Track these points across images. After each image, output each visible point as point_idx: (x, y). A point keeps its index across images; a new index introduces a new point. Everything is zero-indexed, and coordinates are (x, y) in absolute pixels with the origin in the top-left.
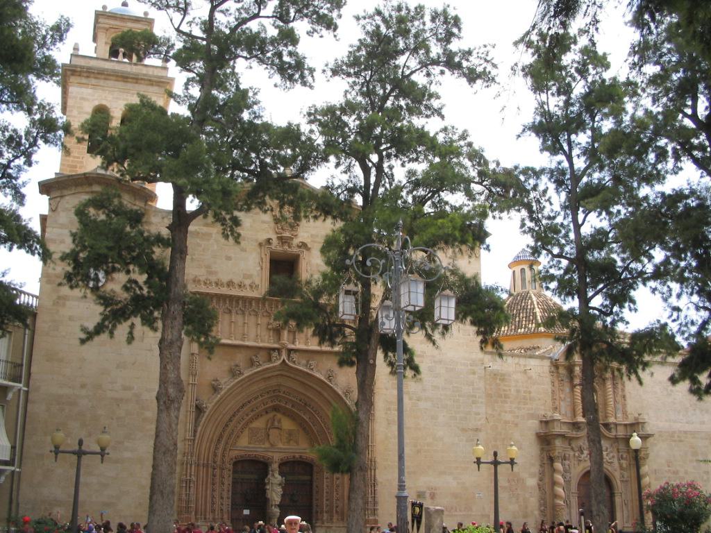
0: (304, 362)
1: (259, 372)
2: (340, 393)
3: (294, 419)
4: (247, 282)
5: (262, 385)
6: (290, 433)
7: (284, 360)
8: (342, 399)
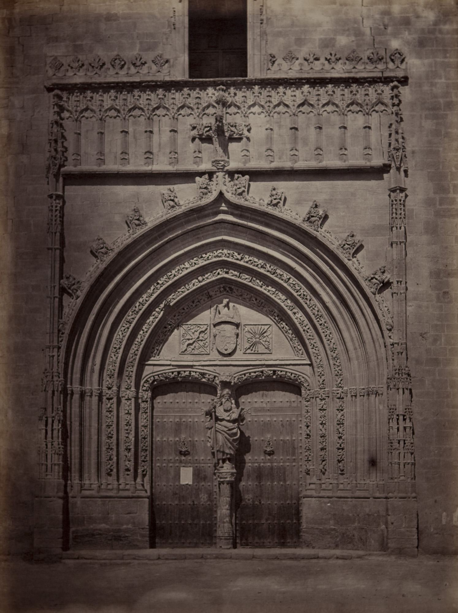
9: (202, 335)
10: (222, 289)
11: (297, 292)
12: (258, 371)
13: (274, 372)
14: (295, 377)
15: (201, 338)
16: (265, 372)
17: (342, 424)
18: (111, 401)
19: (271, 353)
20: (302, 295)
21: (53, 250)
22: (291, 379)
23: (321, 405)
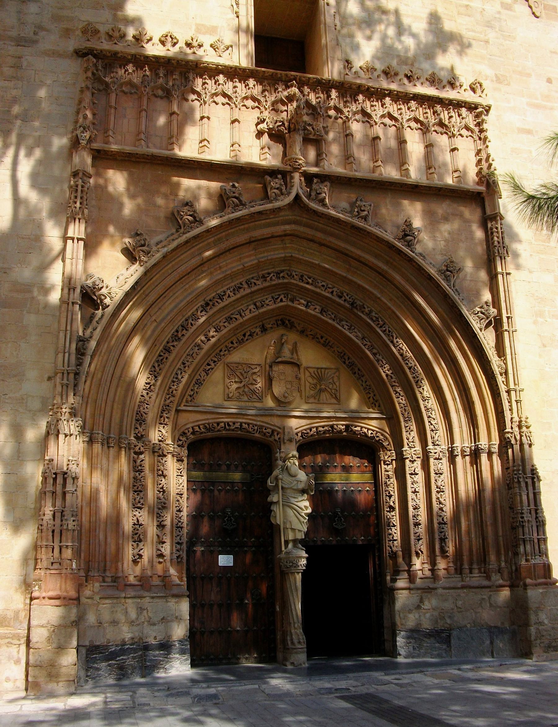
0: (344, 205)
2: (433, 272)
3: (326, 345)
4: (207, 40)
5: (250, 258)
6: (319, 376)
7: (297, 197)
8: (438, 286)
10: (279, 322)
11: (381, 327)
12: (327, 426)
14: (372, 433)
16: (335, 426)
17: (443, 492)
21: (76, 241)
23: (413, 469)
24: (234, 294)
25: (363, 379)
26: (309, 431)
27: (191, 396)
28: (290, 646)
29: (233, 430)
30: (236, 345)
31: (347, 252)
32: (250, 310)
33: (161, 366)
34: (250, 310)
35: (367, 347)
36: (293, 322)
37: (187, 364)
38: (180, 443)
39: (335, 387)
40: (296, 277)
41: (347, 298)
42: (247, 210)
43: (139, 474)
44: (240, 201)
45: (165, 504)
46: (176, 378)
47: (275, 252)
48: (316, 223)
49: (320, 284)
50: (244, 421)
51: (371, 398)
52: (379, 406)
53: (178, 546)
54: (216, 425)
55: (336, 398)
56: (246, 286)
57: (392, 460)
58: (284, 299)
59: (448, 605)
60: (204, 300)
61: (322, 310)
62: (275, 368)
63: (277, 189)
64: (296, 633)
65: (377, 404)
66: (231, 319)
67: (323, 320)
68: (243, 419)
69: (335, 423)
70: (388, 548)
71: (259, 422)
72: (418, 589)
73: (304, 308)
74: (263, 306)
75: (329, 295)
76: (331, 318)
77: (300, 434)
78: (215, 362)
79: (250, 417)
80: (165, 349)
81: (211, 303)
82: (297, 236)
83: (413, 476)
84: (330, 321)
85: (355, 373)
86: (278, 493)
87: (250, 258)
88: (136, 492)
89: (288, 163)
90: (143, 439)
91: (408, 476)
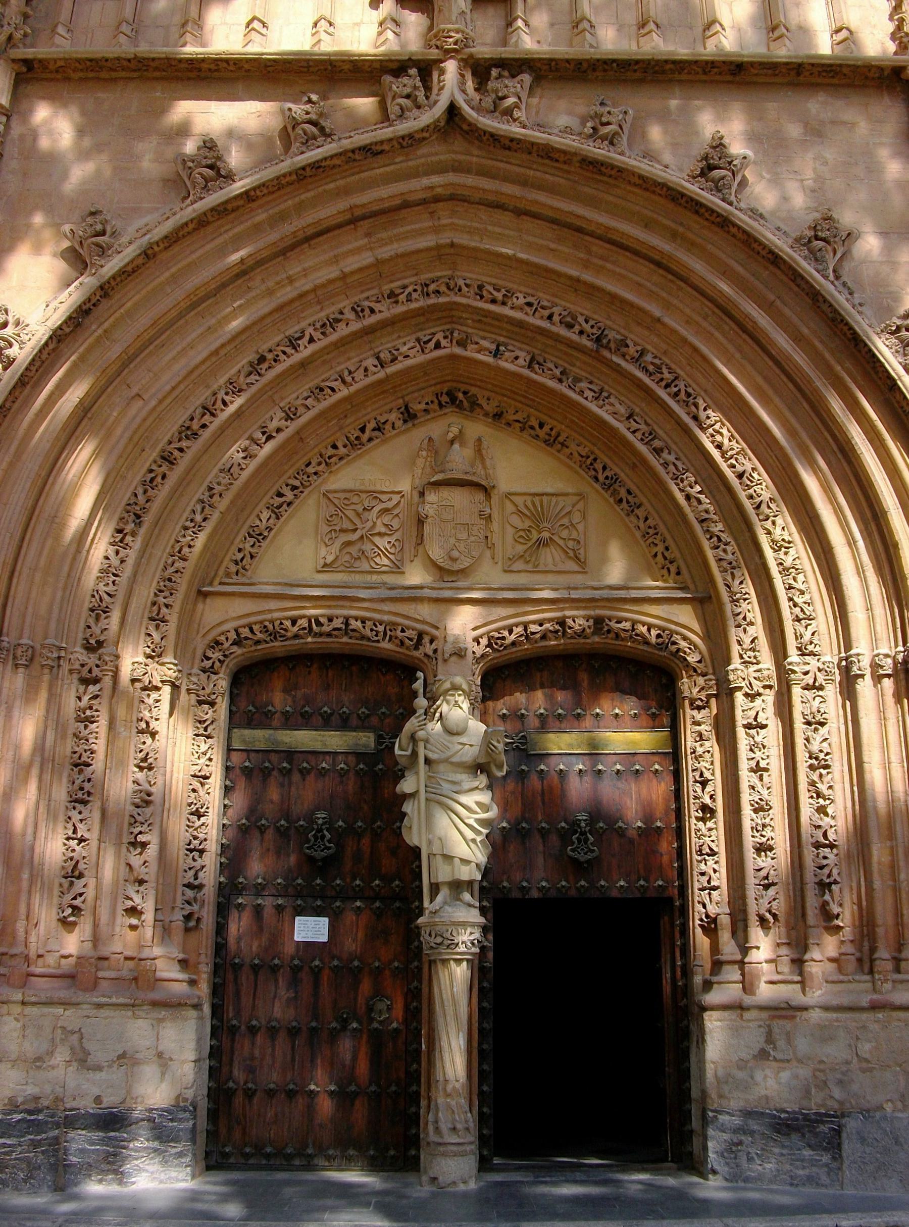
1: (316, 166)
2: (782, 245)
3: (552, 442)
7: (452, 110)
8: (795, 276)
9: (386, 519)
10: (445, 399)
11: (667, 386)
12: (550, 620)
13: (599, 621)
14: (659, 636)
15: (380, 528)
16: (570, 622)
17: (827, 767)
18: (91, 688)
19: (586, 573)
20: (682, 395)
22: (647, 643)
23: (752, 713)
24: (323, 334)
25: (640, 512)
26: (506, 633)
27: (237, 563)
28: (433, 1137)
29: (329, 635)
30: (342, 451)
31: (578, 223)
32: (366, 370)
33: (151, 492)
34: (366, 370)
35: (639, 435)
36: (475, 395)
37: (218, 489)
38: (208, 664)
39: (574, 535)
40: (465, 289)
41: (587, 327)
42: (334, 145)
43: (86, 727)
44: (322, 129)
45: (149, 795)
46: (192, 521)
47: (416, 237)
48: (501, 165)
49: (522, 301)
50: (353, 613)
51: (660, 556)
52: (678, 573)
53: (190, 893)
54: (288, 623)
55: (577, 558)
56: (352, 316)
57: (709, 696)
58: (444, 343)
59: (836, 1052)
60: (257, 352)
61: (532, 359)
62: (431, 497)
63: (408, 97)
64: (449, 1106)
65: (673, 569)
66: (322, 390)
67: (535, 382)
68: (352, 608)
69: (568, 613)
70: (699, 907)
71: (387, 613)
72: (761, 1008)
73: (490, 359)
74: (394, 360)
75: (545, 324)
76: (553, 377)
77: (484, 641)
78: (294, 488)
79: (366, 605)
80: (163, 458)
81: (270, 356)
82: (464, 200)
83: (753, 732)
84: (552, 384)
85: (621, 501)
86: (417, 773)
87: (356, 254)
88: (76, 765)
89: (433, 43)
90: (100, 651)
91: (741, 732)
